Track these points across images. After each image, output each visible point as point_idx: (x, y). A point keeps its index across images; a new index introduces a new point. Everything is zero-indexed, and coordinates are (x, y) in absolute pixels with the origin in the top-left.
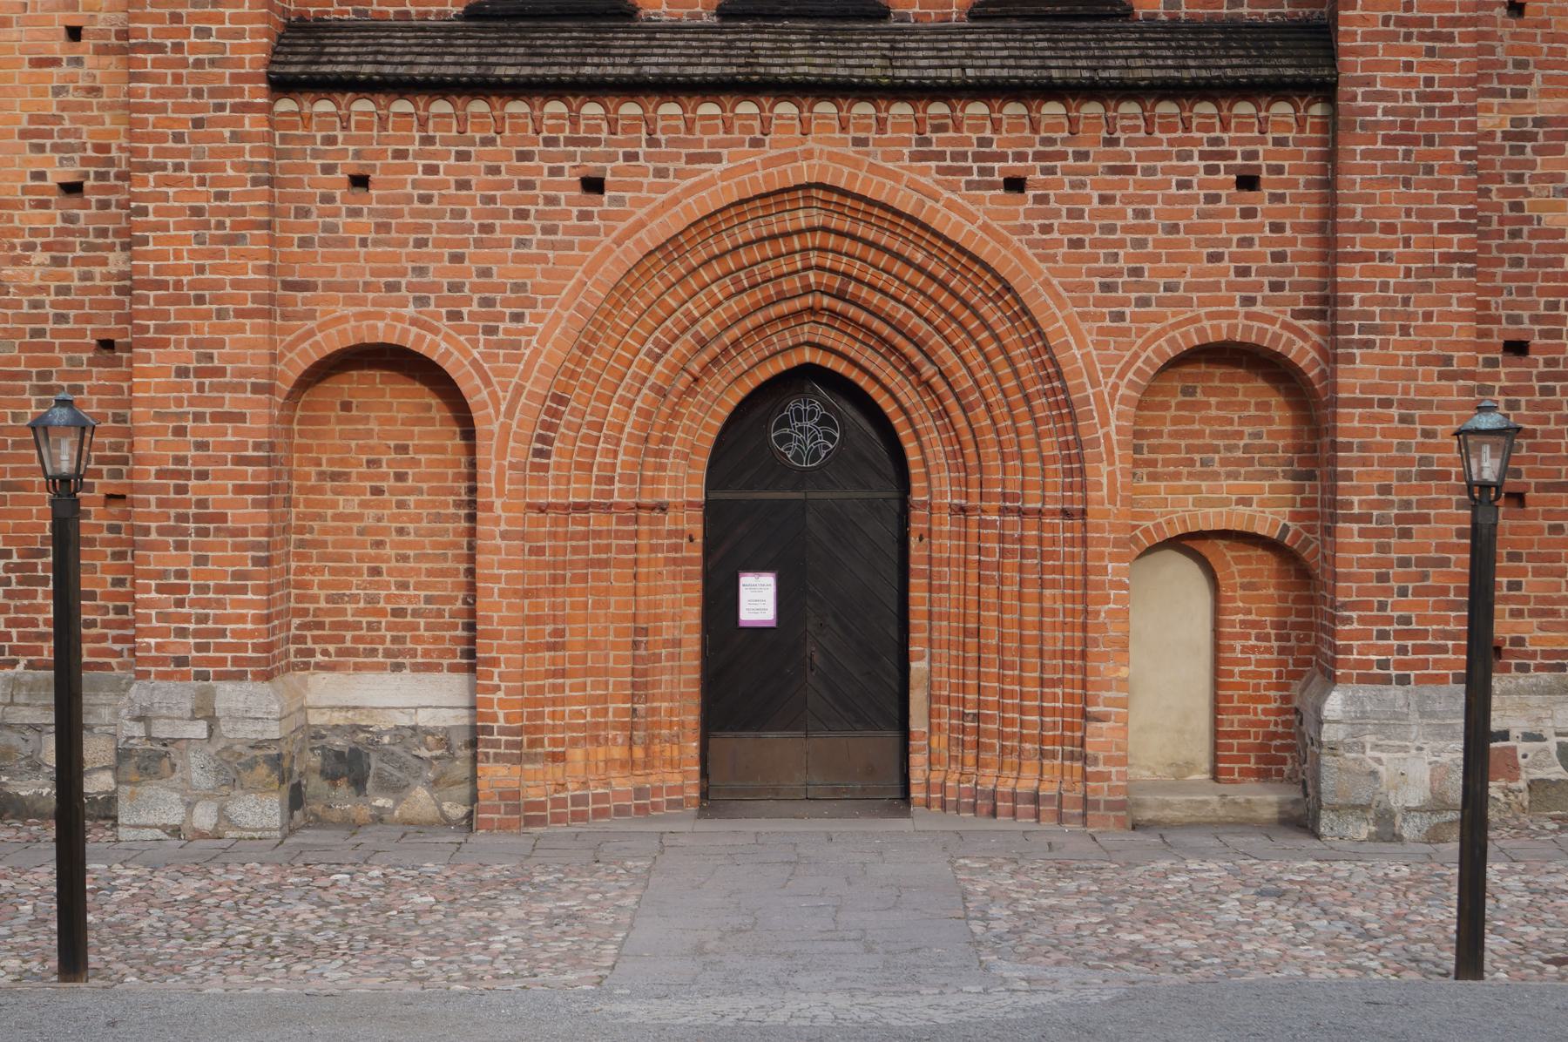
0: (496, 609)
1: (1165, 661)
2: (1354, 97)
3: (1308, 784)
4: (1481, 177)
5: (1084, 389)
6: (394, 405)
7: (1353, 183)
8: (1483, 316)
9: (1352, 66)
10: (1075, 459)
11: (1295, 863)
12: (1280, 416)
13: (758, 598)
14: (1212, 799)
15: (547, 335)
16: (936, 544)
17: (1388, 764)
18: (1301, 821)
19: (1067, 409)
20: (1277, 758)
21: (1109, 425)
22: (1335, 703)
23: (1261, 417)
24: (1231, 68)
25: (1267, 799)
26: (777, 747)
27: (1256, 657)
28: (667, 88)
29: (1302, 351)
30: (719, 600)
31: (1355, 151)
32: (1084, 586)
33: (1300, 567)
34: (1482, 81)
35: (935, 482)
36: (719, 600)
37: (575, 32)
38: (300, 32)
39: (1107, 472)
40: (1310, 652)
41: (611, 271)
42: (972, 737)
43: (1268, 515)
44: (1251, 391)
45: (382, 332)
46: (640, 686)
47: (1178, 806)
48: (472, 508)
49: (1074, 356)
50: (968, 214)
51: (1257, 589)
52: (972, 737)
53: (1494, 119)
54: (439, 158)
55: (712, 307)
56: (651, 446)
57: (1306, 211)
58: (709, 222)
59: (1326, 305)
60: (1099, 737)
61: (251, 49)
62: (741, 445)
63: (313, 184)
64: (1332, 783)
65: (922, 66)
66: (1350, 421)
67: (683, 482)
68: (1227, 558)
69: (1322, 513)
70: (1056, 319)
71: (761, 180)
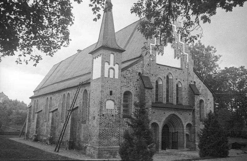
50: (179, 116)
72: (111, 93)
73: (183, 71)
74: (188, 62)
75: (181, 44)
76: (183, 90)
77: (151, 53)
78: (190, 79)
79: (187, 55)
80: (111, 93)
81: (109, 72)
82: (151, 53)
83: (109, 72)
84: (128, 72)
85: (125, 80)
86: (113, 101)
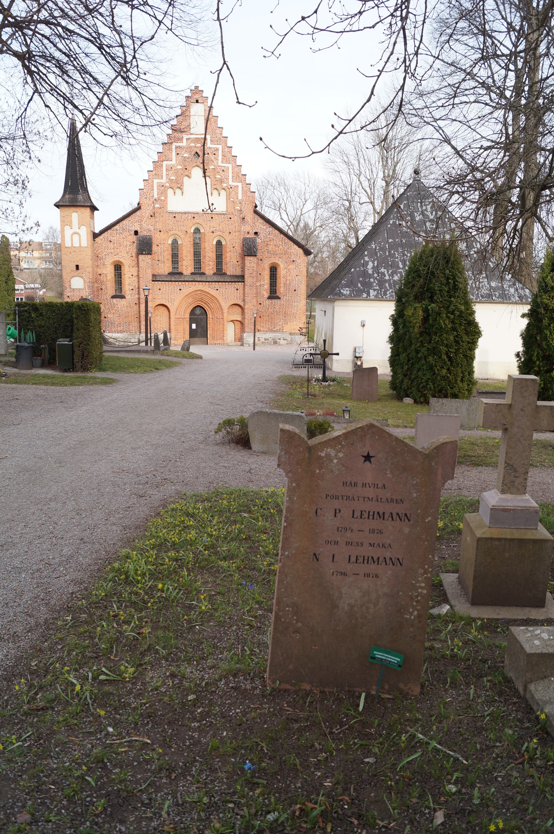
0: (172, 327)
1: (230, 331)
2: (246, 283)
3: (243, 342)
4: (257, 289)
5: (223, 308)
6: (163, 309)
7: (246, 290)
8: (257, 301)
9: (246, 280)
10: (223, 313)
11: (242, 347)
12: (240, 310)
13: (194, 326)
14: (235, 343)
15: (176, 303)
16: (210, 321)
17: (249, 340)
18: (242, 345)
19: (222, 309)
20: (240, 340)
21: (225, 311)
22: (245, 335)
23: (238, 309)
24: (236, 280)
25: (239, 343)
26: (196, 339)
27: (238, 331)
28: (187, 281)
29: (242, 304)
30: (191, 326)
31: (246, 287)
32: (223, 325)
33: (242, 323)
34: (257, 281)
35: (210, 315)
36: (191, 326)
37: (178, 276)
38: (154, 275)
39: (225, 315)
40: (243, 330)
41: (182, 297)
42: (213, 338)
43: (239, 319)
44: (238, 307)
45: (162, 303)
46: (184, 334)
47: (231, 344)
48: (170, 318)
49: (222, 305)
50: (213, 292)
51: (238, 325)
52: (213, 338)
53: (258, 284)
54: (167, 287)
55: (190, 300)
56: (185, 313)
57: (242, 292)
58: (190, 293)
59: (244, 300)
60: (225, 338)
61: (150, 278)
62: (192, 312)
63: (155, 289)
64: (244, 342)
65: (209, 280)
66: (246, 310)
67: (187, 316)
68: (235, 322)
69: (244, 318)
70: (221, 302)
71: (195, 289)
72: (77, 267)
73: (229, 216)
74: (240, 197)
75: (223, 168)
76: (228, 250)
77: (156, 196)
78: (246, 228)
79: (237, 187)
80: (77, 267)
81: (72, 240)
82: (156, 196)
83: (72, 240)
84: (115, 232)
85: (111, 245)
86: (82, 277)
